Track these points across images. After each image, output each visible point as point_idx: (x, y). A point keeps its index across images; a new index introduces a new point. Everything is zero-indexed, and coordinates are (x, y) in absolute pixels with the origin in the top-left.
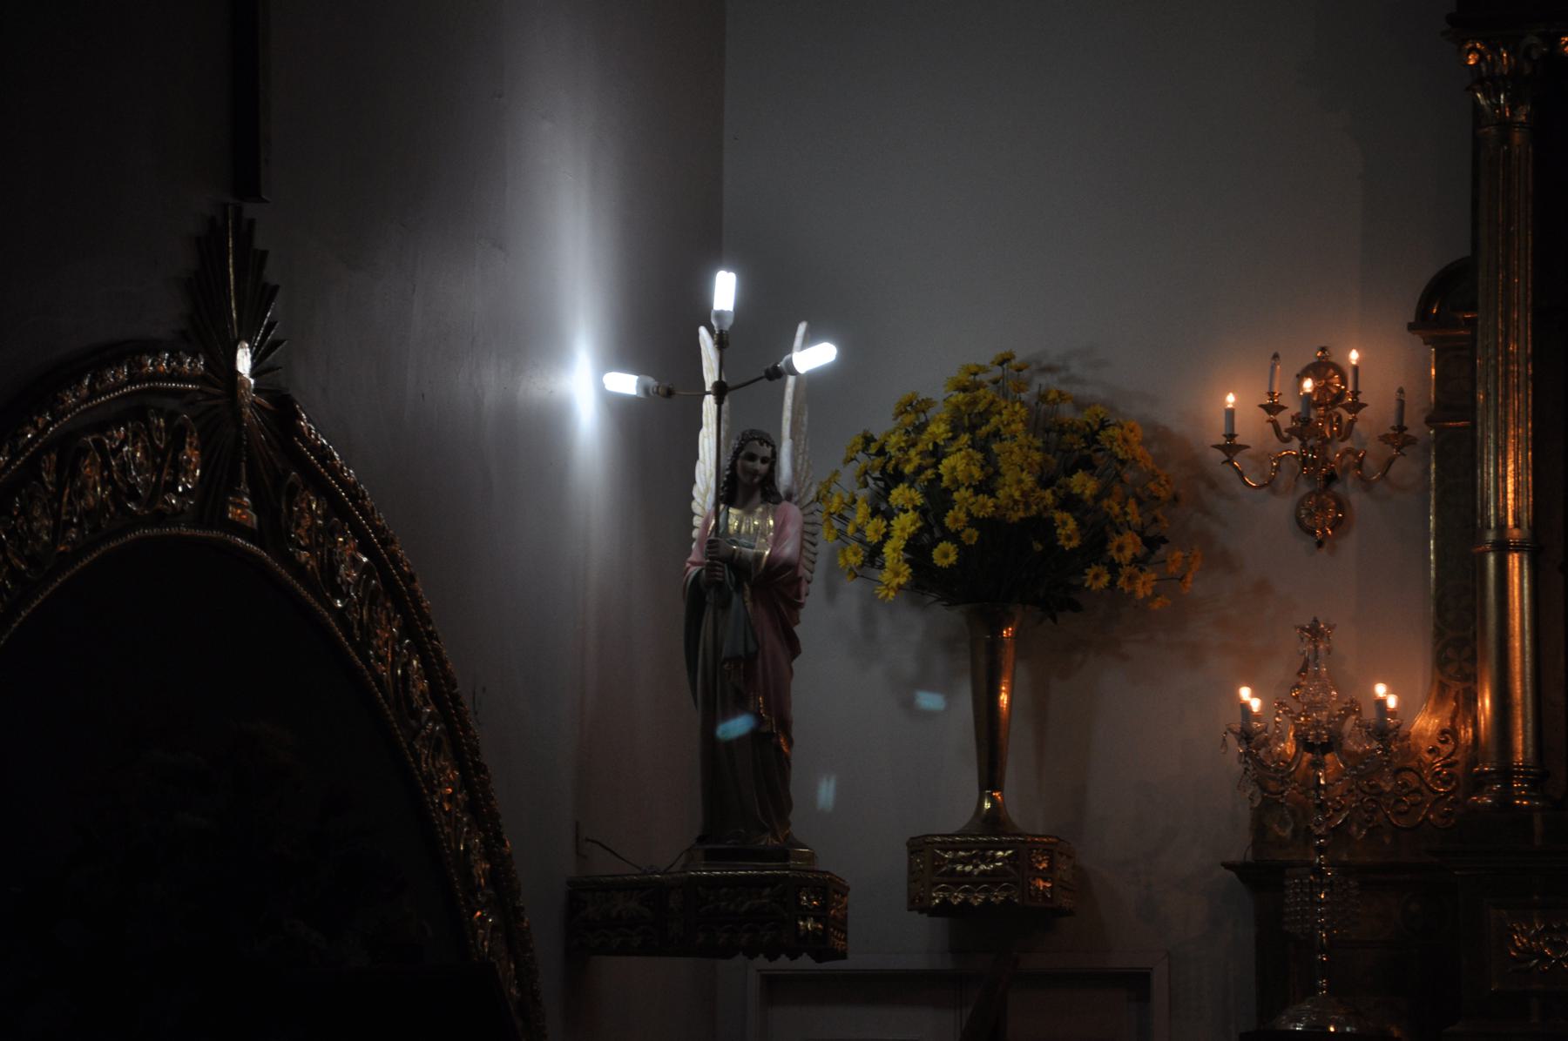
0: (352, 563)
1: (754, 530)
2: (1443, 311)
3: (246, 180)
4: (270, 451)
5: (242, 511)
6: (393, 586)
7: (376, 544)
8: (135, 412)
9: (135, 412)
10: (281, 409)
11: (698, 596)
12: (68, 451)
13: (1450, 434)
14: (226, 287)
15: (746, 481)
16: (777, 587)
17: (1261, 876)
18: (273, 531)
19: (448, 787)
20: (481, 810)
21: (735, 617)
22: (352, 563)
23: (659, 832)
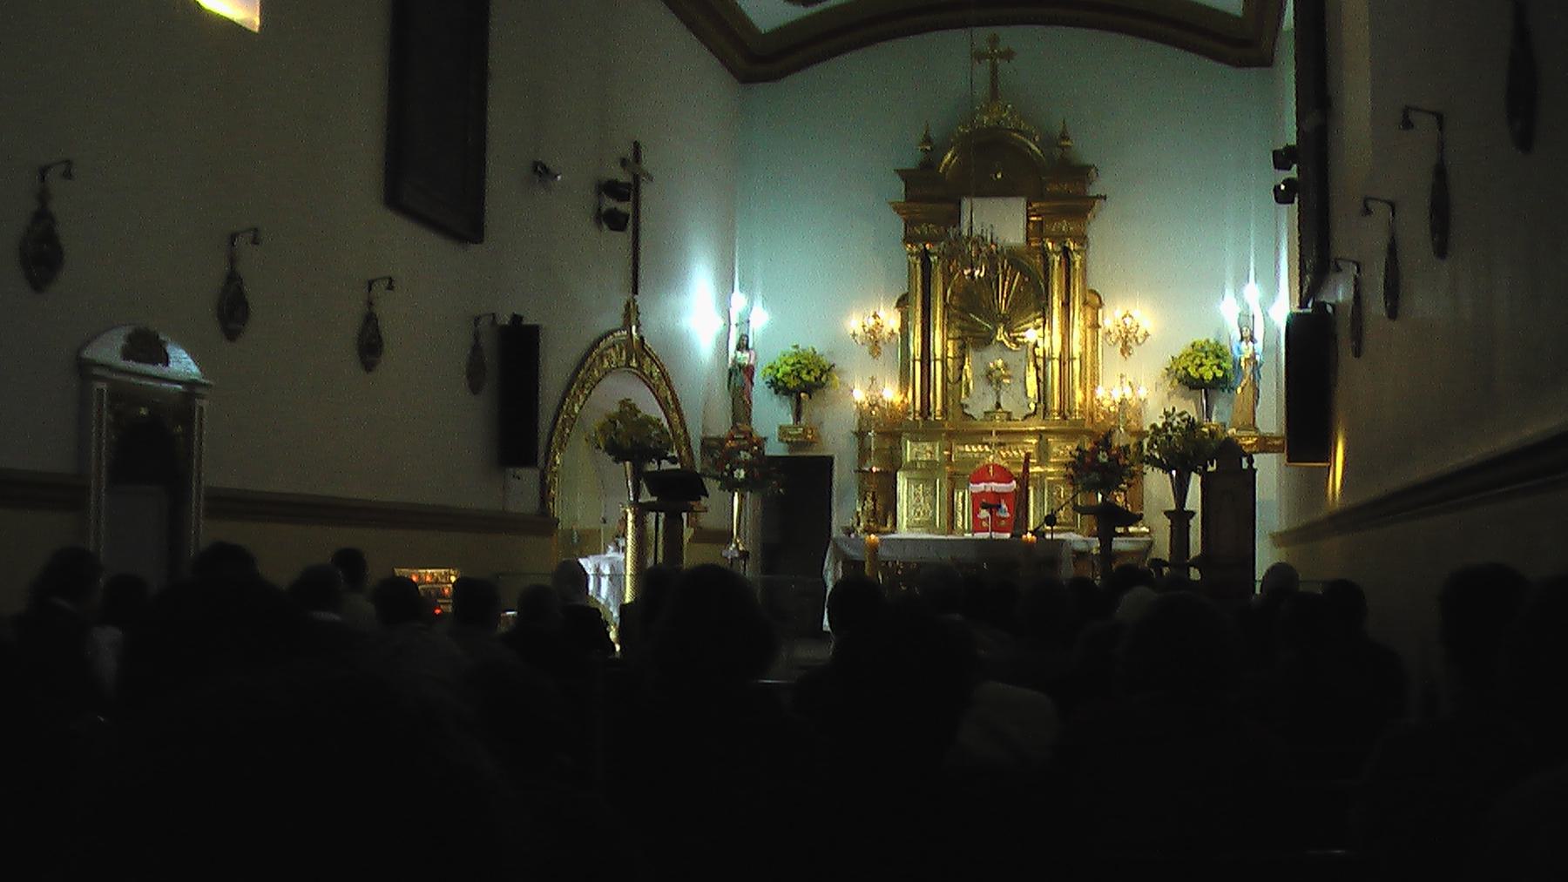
1: (744, 357)
2: (903, 303)
3: (635, 292)
5: (634, 363)
6: (664, 375)
10: (642, 338)
12: (601, 357)
13: (905, 329)
14: (631, 314)
15: (743, 346)
16: (749, 371)
17: (861, 434)
18: (640, 366)
20: (682, 423)
21: (740, 376)
23: (721, 425)
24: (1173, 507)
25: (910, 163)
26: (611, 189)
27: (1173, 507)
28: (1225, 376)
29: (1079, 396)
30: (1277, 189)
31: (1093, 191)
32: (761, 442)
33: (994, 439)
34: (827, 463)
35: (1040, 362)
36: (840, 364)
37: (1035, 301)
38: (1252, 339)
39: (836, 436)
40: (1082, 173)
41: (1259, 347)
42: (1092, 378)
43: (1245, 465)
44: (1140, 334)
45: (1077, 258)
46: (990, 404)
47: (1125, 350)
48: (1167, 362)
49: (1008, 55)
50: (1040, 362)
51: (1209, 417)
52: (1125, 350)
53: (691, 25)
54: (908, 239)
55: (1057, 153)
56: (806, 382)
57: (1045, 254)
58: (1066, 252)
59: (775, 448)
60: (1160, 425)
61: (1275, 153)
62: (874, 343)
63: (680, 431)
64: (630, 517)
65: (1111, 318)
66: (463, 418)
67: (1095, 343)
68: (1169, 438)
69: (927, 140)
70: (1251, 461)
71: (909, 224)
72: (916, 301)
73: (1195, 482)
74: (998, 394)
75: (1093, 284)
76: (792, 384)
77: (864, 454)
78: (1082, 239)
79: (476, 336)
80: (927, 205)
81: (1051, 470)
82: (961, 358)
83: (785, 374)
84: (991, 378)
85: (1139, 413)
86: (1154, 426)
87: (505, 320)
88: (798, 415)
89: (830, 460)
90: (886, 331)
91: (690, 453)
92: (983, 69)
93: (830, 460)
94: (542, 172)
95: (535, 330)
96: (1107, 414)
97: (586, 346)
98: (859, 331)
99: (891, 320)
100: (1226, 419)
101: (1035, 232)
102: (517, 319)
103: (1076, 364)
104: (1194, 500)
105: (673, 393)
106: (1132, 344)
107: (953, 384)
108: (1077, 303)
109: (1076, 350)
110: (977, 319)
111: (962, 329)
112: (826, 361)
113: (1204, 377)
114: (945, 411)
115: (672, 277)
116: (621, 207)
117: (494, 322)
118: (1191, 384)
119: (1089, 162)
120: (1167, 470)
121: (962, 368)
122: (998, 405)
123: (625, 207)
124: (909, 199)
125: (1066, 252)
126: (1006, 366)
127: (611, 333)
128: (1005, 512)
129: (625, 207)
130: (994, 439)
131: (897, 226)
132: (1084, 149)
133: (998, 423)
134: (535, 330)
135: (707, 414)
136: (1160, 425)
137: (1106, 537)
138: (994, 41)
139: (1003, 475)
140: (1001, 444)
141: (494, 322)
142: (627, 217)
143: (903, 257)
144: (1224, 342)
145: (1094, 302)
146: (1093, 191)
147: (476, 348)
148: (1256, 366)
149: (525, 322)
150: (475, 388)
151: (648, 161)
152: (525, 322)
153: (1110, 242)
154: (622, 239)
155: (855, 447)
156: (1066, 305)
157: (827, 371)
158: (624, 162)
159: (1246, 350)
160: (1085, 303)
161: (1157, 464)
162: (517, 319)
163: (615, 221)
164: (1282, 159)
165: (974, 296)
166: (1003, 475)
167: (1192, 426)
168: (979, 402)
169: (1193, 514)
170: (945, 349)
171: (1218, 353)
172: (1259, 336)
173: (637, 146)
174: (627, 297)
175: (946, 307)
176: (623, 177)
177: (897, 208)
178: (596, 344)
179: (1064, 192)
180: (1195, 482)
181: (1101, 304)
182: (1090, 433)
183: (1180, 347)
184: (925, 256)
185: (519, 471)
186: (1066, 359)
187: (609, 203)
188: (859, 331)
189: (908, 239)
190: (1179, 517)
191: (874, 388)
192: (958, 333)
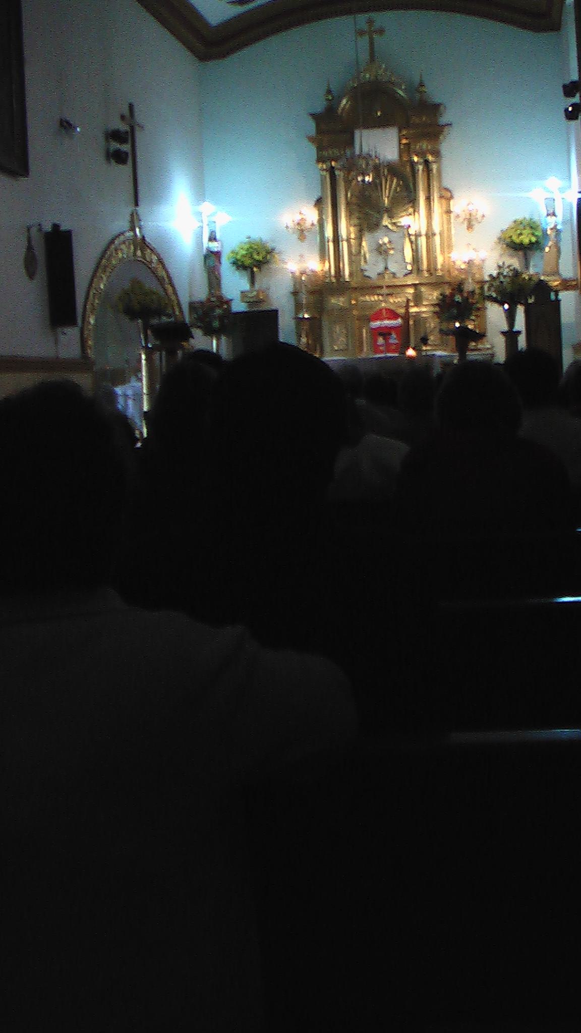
0: (155, 258)
1: (214, 246)
2: (319, 203)
3: (137, 204)
4: (142, 244)
5: (139, 253)
6: (160, 261)
7: (158, 256)
8: (124, 242)
9: (124, 242)
10: (143, 238)
11: (206, 257)
12: (116, 250)
13: (321, 223)
15: (213, 238)
16: (217, 255)
17: (295, 293)
19: (170, 290)
21: (212, 258)
22: (155, 258)
23: (201, 293)
24: (505, 328)
25: (319, 106)
26: (116, 136)
27: (505, 328)
28: (537, 242)
29: (440, 260)
30: (566, 110)
31: (443, 120)
32: (228, 302)
33: (385, 291)
34: (274, 314)
35: (413, 238)
36: (279, 247)
37: (407, 197)
38: (554, 214)
39: (278, 294)
40: (435, 109)
41: (559, 219)
42: (447, 246)
43: (553, 297)
44: (479, 216)
45: (434, 167)
46: (380, 268)
47: (470, 227)
48: (498, 234)
49: (381, 31)
50: (413, 238)
51: (527, 266)
52: (470, 227)
53: (163, 22)
54: (320, 160)
55: (418, 96)
56: (256, 260)
57: (413, 165)
58: (427, 163)
59: (239, 306)
60: (495, 274)
61: (565, 87)
62: (301, 232)
63: (173, 298)
64: (143, 357)
65: (458, 205)
66: (28, 296)
67: (449, 222)
68: (502, 282)
69: (329, 92)
70: (557, 295)
71: (320, 149)
72: (328, 201)
73: (520, 311)
74: (386, 260)
75: (446, 183)
76: (248, 262)
77: (298, 307)
78: (437, 154)
79: (29, 240)
80: (332, 135)
81: (424, 309)
82: (360, 238)
83: (243, 256)
84: (381, 251)
85: (481, 268)
86: (491, 276)
87: (48, 228)
88: (252, 281)
89: (275, 312)
90: (308, 224)
91: (181, 311)
92: (364, 41)
93: (275, 312)
94: (66, 126)
95: (68, 235)
96: (460, 270)
97: (104, 244)
98: (291, 225)
99: (311, 215)
100: (537, 270)
101: (405, 150)
102: (56, 227)
103: (437, 239)
104: (520, 323)
105: (167, 272)
106: (473, 223)
107: (356, 256)
108: (436, 196)
109: (436, 228)
110: (369, 213)
111: (359, 218)
112: (270, 245)
113: (524, 244)
114: (351, 274)
115: (160, 194)
116: (123, 147)
117: (40, 230)
118: (515, 247)
119: (437, 100)
120: (502, 304)
121: (360, 245)
122: (386, 268)
123: (126, 148)
124: (319, 131)
125: (427, 163)
126: (390, 242)
127: (122, 233)
128: (394, 339)
129: (126, 148)
130: (385, 291)
131: (311, 150)
132: (435, 92)
133: (388, 280)
134: (68, 235)
135: (190, 286)
136: (495, 274)
137: (462, 348)
138: (370, 22)
139: (393, 315)
140: (388, 295)
141: (40, 230)
142: (127, 154)
143: (318, 171)
144: (536, 218)
145: (447, 196)
146: (443, 120)
147: (30, 248)
148: (558, 232)
149: (63, 228)
150: (31, 275)
151: (139, 117)
152: (63, 228)
153: (456, 155)
154: (125, 170)
155: (292, 303)
156: (428, 199)
157: (270, 252)
158: (123, 117)
159: (551, 221)
160: (441, 197)
161: (495, 300)
162: (56, 227)
163: (119, 158)
164: (570, 90)
165: (367, 197)
166: (393, 315)
167: (516, 274)
168: (373, 267)
169: (519, 332)
170: (349, 234)
171: (532, 226)
172: (559, 212)
173: (131, 107)
174: (131, 208)
175: (348, 204)
176: (123, 127)
177: (311, 139)
178: (112, 242)
179: (423, 122)
180: (520, 311)
181: (452, 197)
182: (449, 283)
183: (505, 223)
184: (332, 170)
185: (65, 330)
186: (430, 235)
187: (115, 145)
188: (291, 225)
189: (320, 160)
190: (511, 336)
191: (301, 262)
192: (356, 221)
